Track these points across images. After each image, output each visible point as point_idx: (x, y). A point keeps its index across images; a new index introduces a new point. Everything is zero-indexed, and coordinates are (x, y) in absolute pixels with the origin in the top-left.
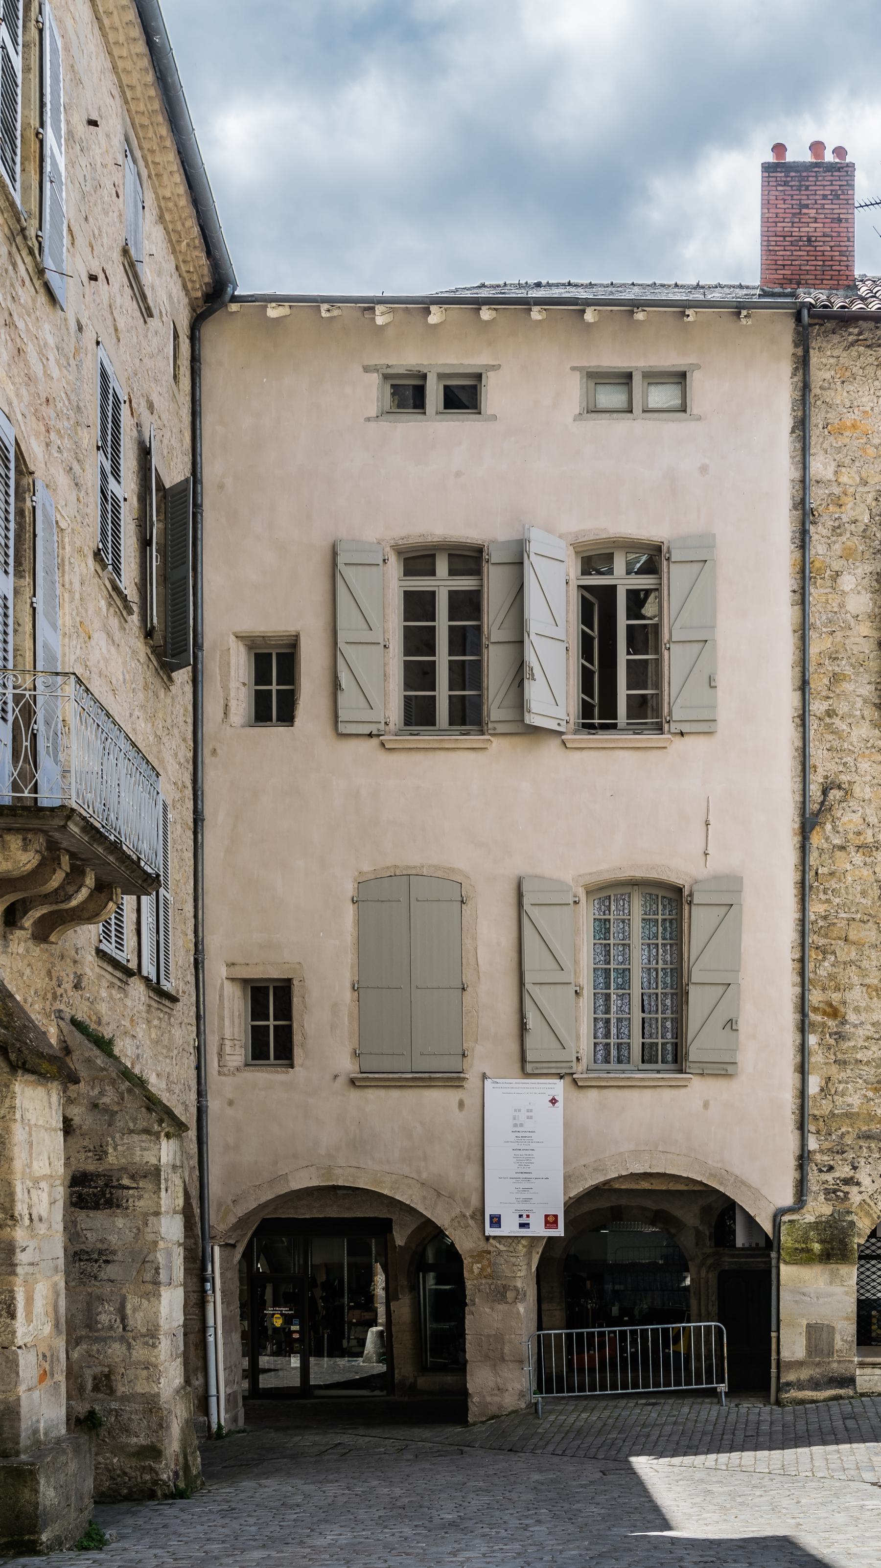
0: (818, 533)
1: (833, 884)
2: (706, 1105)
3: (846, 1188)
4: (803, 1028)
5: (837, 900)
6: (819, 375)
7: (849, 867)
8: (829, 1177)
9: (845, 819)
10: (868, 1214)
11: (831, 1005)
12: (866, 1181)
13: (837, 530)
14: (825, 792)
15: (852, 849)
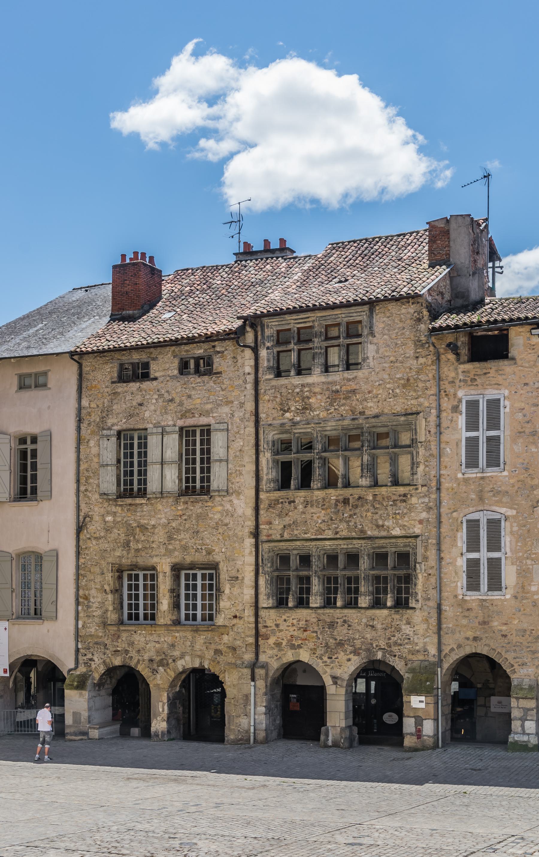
1: (86, 552)
2: (48, 631)
3: (90, 662)
4: (78, 603)
5: (88, 558)
7: (91, 545)
8: (85, 658)
9: (90, 528)
10: (97, 672)
11: (85, 595)
12: (96, 660)
14: (85, 518)
15: (92, 539)
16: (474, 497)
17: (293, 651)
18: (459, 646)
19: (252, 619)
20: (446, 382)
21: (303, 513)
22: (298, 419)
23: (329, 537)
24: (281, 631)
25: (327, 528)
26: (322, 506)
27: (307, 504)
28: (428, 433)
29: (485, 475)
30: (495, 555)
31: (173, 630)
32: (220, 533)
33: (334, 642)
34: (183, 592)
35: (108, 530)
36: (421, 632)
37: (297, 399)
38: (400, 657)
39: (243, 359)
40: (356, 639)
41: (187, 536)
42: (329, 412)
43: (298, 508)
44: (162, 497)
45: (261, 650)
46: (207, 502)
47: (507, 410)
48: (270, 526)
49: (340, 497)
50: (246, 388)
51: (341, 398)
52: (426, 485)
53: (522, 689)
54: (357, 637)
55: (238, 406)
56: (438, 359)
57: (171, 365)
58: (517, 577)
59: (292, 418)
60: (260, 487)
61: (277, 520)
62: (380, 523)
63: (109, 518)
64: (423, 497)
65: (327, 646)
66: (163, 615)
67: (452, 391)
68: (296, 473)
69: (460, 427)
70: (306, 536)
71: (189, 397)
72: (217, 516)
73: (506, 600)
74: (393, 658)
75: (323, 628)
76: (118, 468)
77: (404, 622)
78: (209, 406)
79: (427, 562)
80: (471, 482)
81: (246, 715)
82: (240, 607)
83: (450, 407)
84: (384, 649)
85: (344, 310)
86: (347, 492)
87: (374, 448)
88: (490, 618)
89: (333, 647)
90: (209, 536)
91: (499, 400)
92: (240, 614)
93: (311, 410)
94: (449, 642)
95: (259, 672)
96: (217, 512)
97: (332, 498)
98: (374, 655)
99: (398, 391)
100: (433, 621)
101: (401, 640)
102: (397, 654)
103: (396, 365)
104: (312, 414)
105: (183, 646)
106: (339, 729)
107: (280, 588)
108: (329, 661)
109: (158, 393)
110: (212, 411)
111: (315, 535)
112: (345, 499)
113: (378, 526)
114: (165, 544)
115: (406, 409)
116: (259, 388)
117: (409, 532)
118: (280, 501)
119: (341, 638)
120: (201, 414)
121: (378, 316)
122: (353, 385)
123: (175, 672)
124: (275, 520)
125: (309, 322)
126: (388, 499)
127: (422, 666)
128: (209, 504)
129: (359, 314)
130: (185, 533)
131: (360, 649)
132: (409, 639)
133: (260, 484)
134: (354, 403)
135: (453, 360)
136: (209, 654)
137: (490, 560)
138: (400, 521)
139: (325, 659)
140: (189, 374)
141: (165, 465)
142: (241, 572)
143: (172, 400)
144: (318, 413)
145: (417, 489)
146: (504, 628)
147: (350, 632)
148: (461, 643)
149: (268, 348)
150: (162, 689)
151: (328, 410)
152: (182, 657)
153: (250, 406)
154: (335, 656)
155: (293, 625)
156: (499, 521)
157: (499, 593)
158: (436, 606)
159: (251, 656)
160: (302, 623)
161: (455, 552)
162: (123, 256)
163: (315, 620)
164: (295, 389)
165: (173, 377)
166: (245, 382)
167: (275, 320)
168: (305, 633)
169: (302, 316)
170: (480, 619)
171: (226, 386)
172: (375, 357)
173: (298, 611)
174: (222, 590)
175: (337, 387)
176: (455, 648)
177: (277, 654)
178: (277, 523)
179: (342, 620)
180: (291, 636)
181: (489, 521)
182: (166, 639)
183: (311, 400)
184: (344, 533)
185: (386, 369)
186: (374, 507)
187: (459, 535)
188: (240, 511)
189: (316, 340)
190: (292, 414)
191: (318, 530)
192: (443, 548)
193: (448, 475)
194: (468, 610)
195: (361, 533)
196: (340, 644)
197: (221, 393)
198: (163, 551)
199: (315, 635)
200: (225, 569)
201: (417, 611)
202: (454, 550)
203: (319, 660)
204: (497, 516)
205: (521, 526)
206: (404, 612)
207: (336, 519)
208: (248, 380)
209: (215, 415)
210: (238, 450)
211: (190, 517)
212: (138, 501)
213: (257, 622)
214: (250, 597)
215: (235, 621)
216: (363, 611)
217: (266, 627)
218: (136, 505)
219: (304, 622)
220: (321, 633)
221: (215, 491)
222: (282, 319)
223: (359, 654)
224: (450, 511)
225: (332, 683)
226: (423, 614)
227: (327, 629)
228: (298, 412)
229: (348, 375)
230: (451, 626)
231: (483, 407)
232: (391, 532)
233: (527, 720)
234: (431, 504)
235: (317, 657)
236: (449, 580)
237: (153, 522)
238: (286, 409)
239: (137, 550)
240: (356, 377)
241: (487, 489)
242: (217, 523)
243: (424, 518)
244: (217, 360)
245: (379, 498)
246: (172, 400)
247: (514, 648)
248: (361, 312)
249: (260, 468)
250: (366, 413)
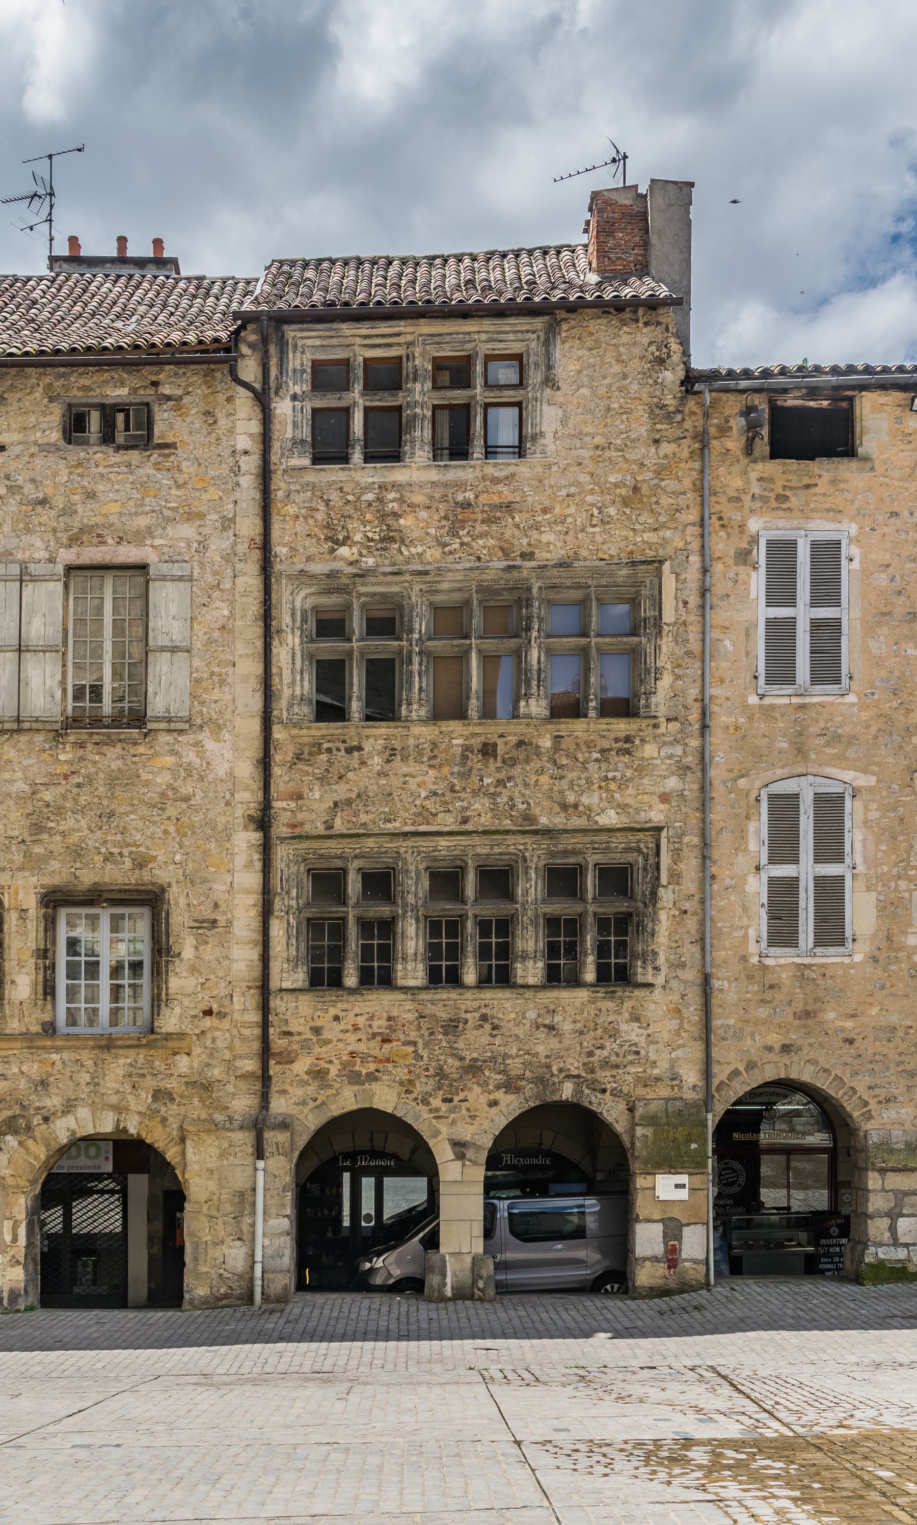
16: (785, 745)
17: (357, 1087)
18: (751, 1066)
19: (255, 1017)
20: (723, 499)
21: (382, 774)
22: (371, 561)
23: (447, 829)
24: (327, 1042)
25: (442, 809)
26: (430, 759)
27: (391, 754)
28: (681, 605)
29: (807, 700)
30: (831, 870)
31: (43, 1048)
32: (169, 818)
33: (457, 1063)
34: (62, 958)
36: (665, 1036)
37: (368, 516)
38: (616, 1093)
39: (232, 418)
40: (511, 1057)
41: (83, 824)
42: (447, 549)
43: (369, 762)
44: (19, 731)
45: (274, 1088)
46: (135, 744)
47: (856, 565)
48: (300, 802)
49: (473, 741)
50: (238, 484)
51: (476, 521)
52: (676, 719)
53: (891, 1151)
54: (514, 1051)
55: (218, 524)
57: (41, 419)
58: (878, 917)
59: (355, 557)
60: (275, 713)
61: (316, 788)
62: (571, 798)
64: (671, 743)
65: (440, 1074)
66: (16, 1011)
67: (737, 517)
69: (753, 595)
70: (389, 825)
71: (91, 495)
72: (163, 779)
73: (853, 966)
74: (599, 1096)
75: (432, 1034)
77: (626, 1016)
78: (143, 522)
79: (678, 884)
80: (777, 715)
81: (239, 1239)
83: (732, 552)
84: (579, 1076)
85: (488, 325)
86: (489, 731)
88: (819, 1004)
89: (455, 1076)
90: (140, 824)
91: (839, 543)
92: (222, 1005)
93: (402, 542)
95: (273, 1137)
96: (162, 768)
97: (455, 742)
98: (553, 1092)
99: (612, 511)
100: (692, 1012)
101: (617, 1055)
102: (608, 1086)
103: (607, 454)
104: (406, 553)
105: (71, 1084)
106: (469, 1259)
107: (314, 948)
108: (444, 1107)
109: (7, 483)
110: (150, 531)
111: (413, 824)
112: (485, 745)
113: (564, 807)
114: (23, 841)
115: (632, 553)
116: (273, 487)
117: (638, 818)
118: (326, 746)
119: (475, 1055)
120: (121, 538)
121: (567, 345)
122: (506, 493)
123: (47, 1146)
124: (311, 790)
125: (399, 344)
126: (589, 747)
127: (670, 1109)
128: (141, 749)
129: (520, 336)
130: (79, 817)
131: (522, 1077)
132: (637, 1053)
133: (274, 705)
134: (508, 533)
135: (739, 453)
136: (140, 1101)
137: (820, 881)
138: (617, 796)
139: (436, 1102)
140: (85, 442)
141: (28, 655)
142: (223, 907)
143: (43, 502)
144: (420, 549)
145: (656, 726)
146: (849, 1024)
147: (497, 1041)
148: (754, 1058)
149: (294, 398)
150: (13, 1187)
151: (446, 545)
152: (69, 1107)
153: (250, 526)
154: (461, 1096)
155: (356, 1028)
156: (841, 798)
157: (840, 949)
158: (698, 981)
159: (249, 1103)
160: (379, 1024)
161: (743, 863)
163: (411, 1016)
164: (361, 494)
166: (236, 470)
167: (314, 334)
168: (387, 1046)
169: (384, 328)
170: (799, 1006)
171: (186, 476)
172: (560, 433)
173: (370, 997)
174: (175, 949)
175: (467, 494)
176: (741, 1069)
177: (315, 1095)
178: (317, 795)
179: (477, 1015)
180: (351, 1053)
181: (820, 799)
182: (24, 1068)
183: (402, 521)
184: (483, 820)
185: (585, 462)
186: (555, 762)
187: (752, 826)
188: (221, 769)
190: (355, 549)
191: (420, 814)
193: (727, 699)
194: (771, 987)
195: (524, 820)
196: (473, 1069)
197: (174, 492)
198: (18, 858)
199: (410, 1049)
200: (182, 901)
201: (658, 992)
202: (740, 858)
203: (421, 1107)
204: (838, 789)
205: (886, 809)
206: (627, 994)
207: (464, 789)
208: (244, 468)
209: (157, 542)
210: (216, 626)
211: (90, 779)
213: (265, 1025)
214: (247, 966)
215: (208, 1022)
216: (529, 994)
217: (288, 1034)
219: (383, 1023)
220: (426, 1045)
221: (158, 719)
222: (332, 333)
223: (518, 1090)
224: (731, 775)
225: (452, 1156)
226: (670, 998)
227: (440, 1037)
228: (369, 547)
230: (732, 1022)
232: (597, 818)
233: (903, 1216)
234: (690, 759)
235: (416, 1099)
236: (728, 924)
238: (341, 537)
240: (513, 475)
241: (814, 730)
242: (163, 795)
243: (673, 791)
244: (162, 417)
245: (567, 743)
246: (43, 502)
247: (870, 1066)
248: (527, 331)
249: (274, 670)
250: (537, 555)
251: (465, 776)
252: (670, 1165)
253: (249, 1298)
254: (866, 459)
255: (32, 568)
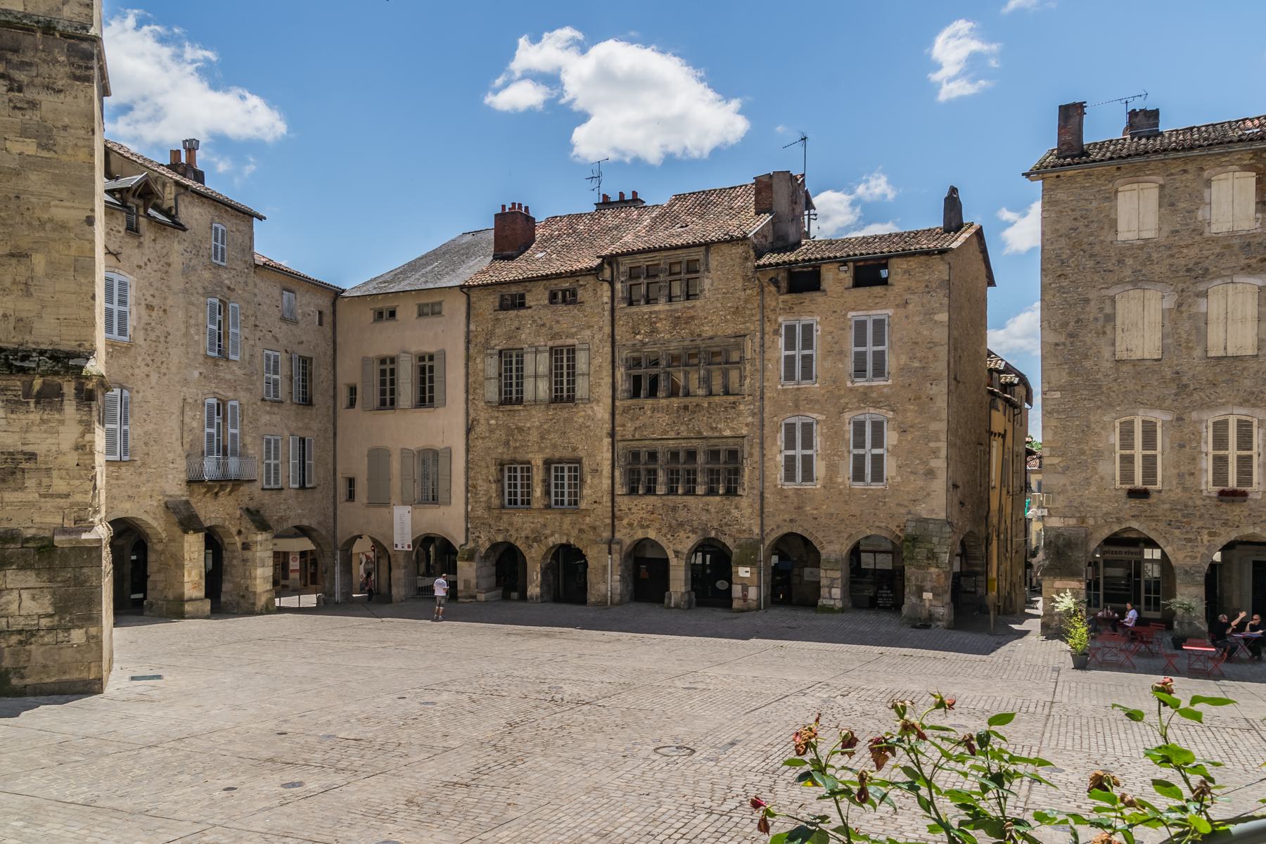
0: (471, 347)
4: (467, 491)
6: (473, 300)
13: (476, 345)
18: (778, 527)
19: (609, 504)
21: (651, 417)
27: (654, 410)
34: (553, 482)
35: (492, 431)
36: (747, 515)
45: (617, 529)
47: (819, 333)
56: (762, 291)
63: (493, 422)
65: (670, 526)
67: (774, 317)
68: (645, 384)
71: (558, 322)
76: (500, 381)
78: (574, 330)
82: (600, 495)
85: (685, 251)
86: (687, 400)
87: (709, 364)
94: (770, 523)
95: (615, 547)
100: (757, 506)
110: (576, 333)
113: (712, 428)
122: (692, 313)
136: (575, 533)
137: (804, 457)
139: (669, 536)
140: (556, 303)
143: (543, 325)
152: (552, 534)
153: (607, 329)
156: (812, 424)
160: (650, 507)
162: (504, 207)
165: (545, 306)
166: (603, 310)
170: (796, 505)
181: (804, 425)
187: (779, 436)
188: (599, 416)
189: (662, 275)
192: (765, 446)
196: (681, 525)
198: (536, 448)
205: (829, 429)
212: (516, 407)
213: (613, 507)
215: (595, 506)
218: (515, 411)
223: (696, 533)
229: (688, 304)
231: (799, 330)
237: (528, 425)
239: (516, 448)
241: (802, 398)
244: (580, 292)
246: (543, 325)
251: (678, 417)
252: (744, 565)
253: (606, 602)
254: (824, 291)
255: (540, 348)
